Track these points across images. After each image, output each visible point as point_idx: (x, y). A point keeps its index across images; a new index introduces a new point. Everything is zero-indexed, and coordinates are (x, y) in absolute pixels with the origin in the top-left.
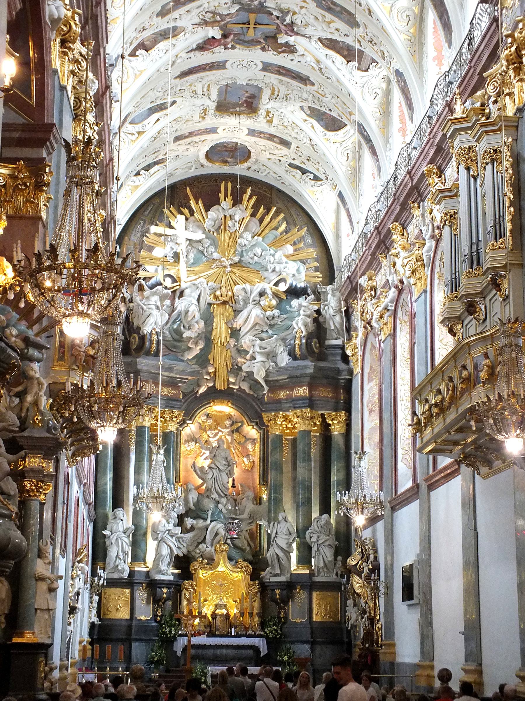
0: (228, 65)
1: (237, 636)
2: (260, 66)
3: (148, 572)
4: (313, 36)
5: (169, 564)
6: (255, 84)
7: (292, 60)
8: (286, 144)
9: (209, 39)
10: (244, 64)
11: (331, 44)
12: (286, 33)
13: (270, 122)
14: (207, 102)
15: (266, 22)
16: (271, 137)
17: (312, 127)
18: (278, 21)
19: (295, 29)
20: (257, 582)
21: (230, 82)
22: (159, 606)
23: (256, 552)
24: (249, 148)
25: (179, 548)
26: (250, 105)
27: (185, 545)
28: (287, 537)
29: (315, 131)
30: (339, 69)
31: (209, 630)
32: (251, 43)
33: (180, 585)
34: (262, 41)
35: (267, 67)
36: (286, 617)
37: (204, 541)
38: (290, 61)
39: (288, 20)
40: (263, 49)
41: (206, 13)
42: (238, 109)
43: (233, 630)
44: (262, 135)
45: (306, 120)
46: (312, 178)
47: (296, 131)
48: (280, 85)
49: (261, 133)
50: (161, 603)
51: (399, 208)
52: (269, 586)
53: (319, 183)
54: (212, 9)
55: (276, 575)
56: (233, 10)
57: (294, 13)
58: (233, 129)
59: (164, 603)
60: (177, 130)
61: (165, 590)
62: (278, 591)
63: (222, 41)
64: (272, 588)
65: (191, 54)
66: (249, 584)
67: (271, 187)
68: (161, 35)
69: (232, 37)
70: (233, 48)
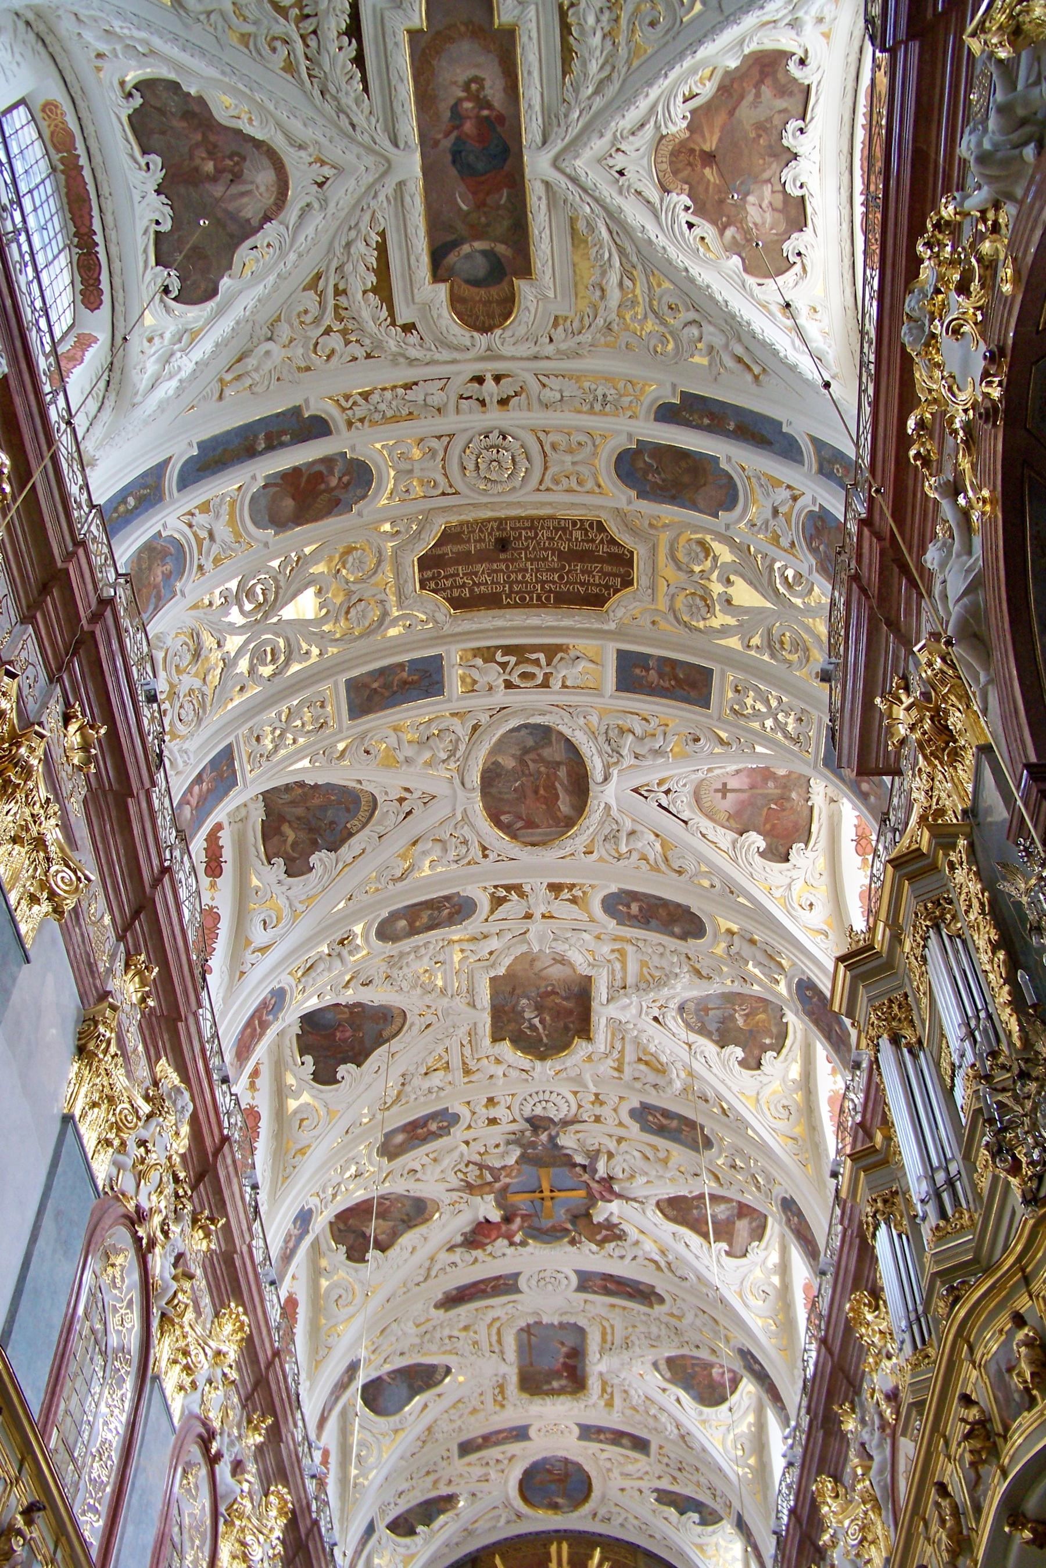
0: (522, 1283)
2: (574, 1280)
4: (646, 1197)
6: (572, 1321)
7: (622, 1257)
8: (641, 1445)
9: (480, 1223)
10: (548, 1276)
11: (680, 1210)
12: (604, 1199)
13: (610, 1404)
14: (504, 1369)
15: (569, 1184)
16: (617, 1437)
17: (678, 1400)
18: (586, 1177)
19: (616, 1188)
21: (531, 1321)
24: (586, 1468)
26: (572, 1376)
29: (683, 1407)
30: (697, 1257)
32: (550, 1235)
34: (569, 1226)
35: (587, 1282)
38: (619, 1261)
39: (602, 1170)
40: (573, 1242)
41: (467, 1166)
42: (555, 1384)
44: (602, 1437)
45: (664, 1390)
46: (697, 1521)
47: (652, 1412)
48: (611, 1316)
49: (600, 1430)
51: (821, 1433)
53: (710, 1528)
54: (477, 1158)
56: (511, 1160)
57: (610, 1155)
58: (554, 1427)
60: (460, 1429)
63: (504, 1228)
65: (457, 1256)
67: (634, 1548)
68: (403, 1221)
69: (518, 1220)
70: (523, 1244)
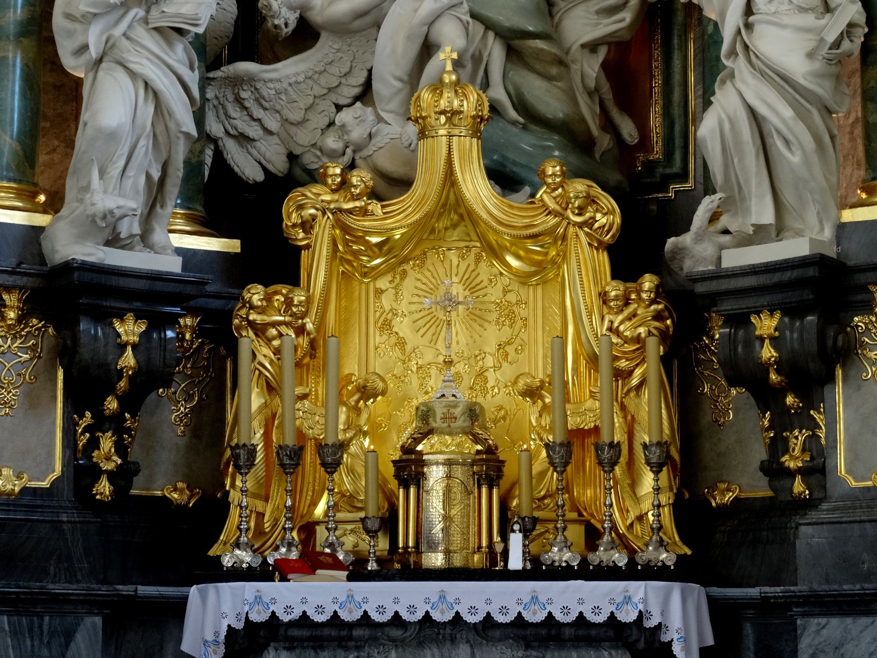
1: (538, 570)
3: (38, 231)
5: (156, 193)
20: (648, 282)
22: (101, 423)
23: (650, 166)
25: (243, 139)
27: (273, 124)
28: (809, 20)
31: (383, 544)
33: (228, 315)
36: (817, 469)
37: (365, 94)
43: (516, 540)
50: (112, 404)
52: (713, 298)
55: (760, 235)
59: (132, 402)
61: (130, 329)
62: (766, 324)
64: (728, 306)
66: (604, 297)
